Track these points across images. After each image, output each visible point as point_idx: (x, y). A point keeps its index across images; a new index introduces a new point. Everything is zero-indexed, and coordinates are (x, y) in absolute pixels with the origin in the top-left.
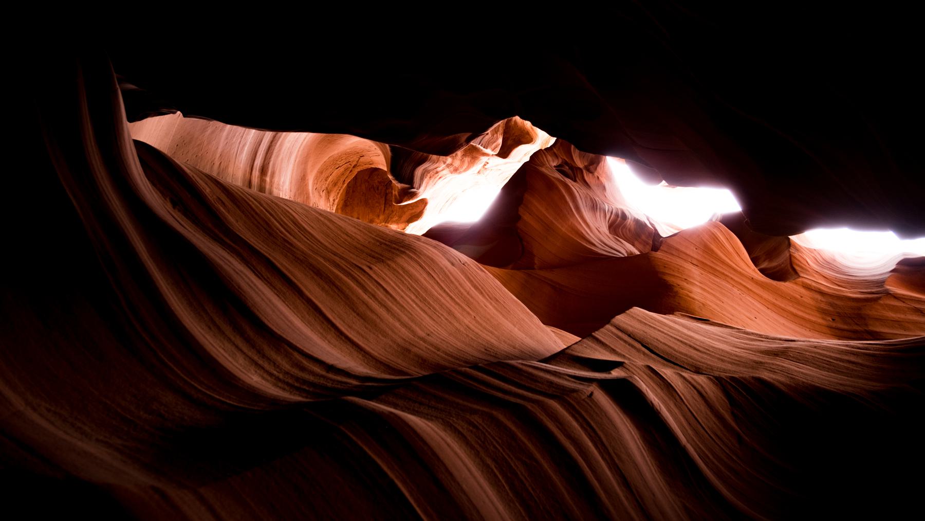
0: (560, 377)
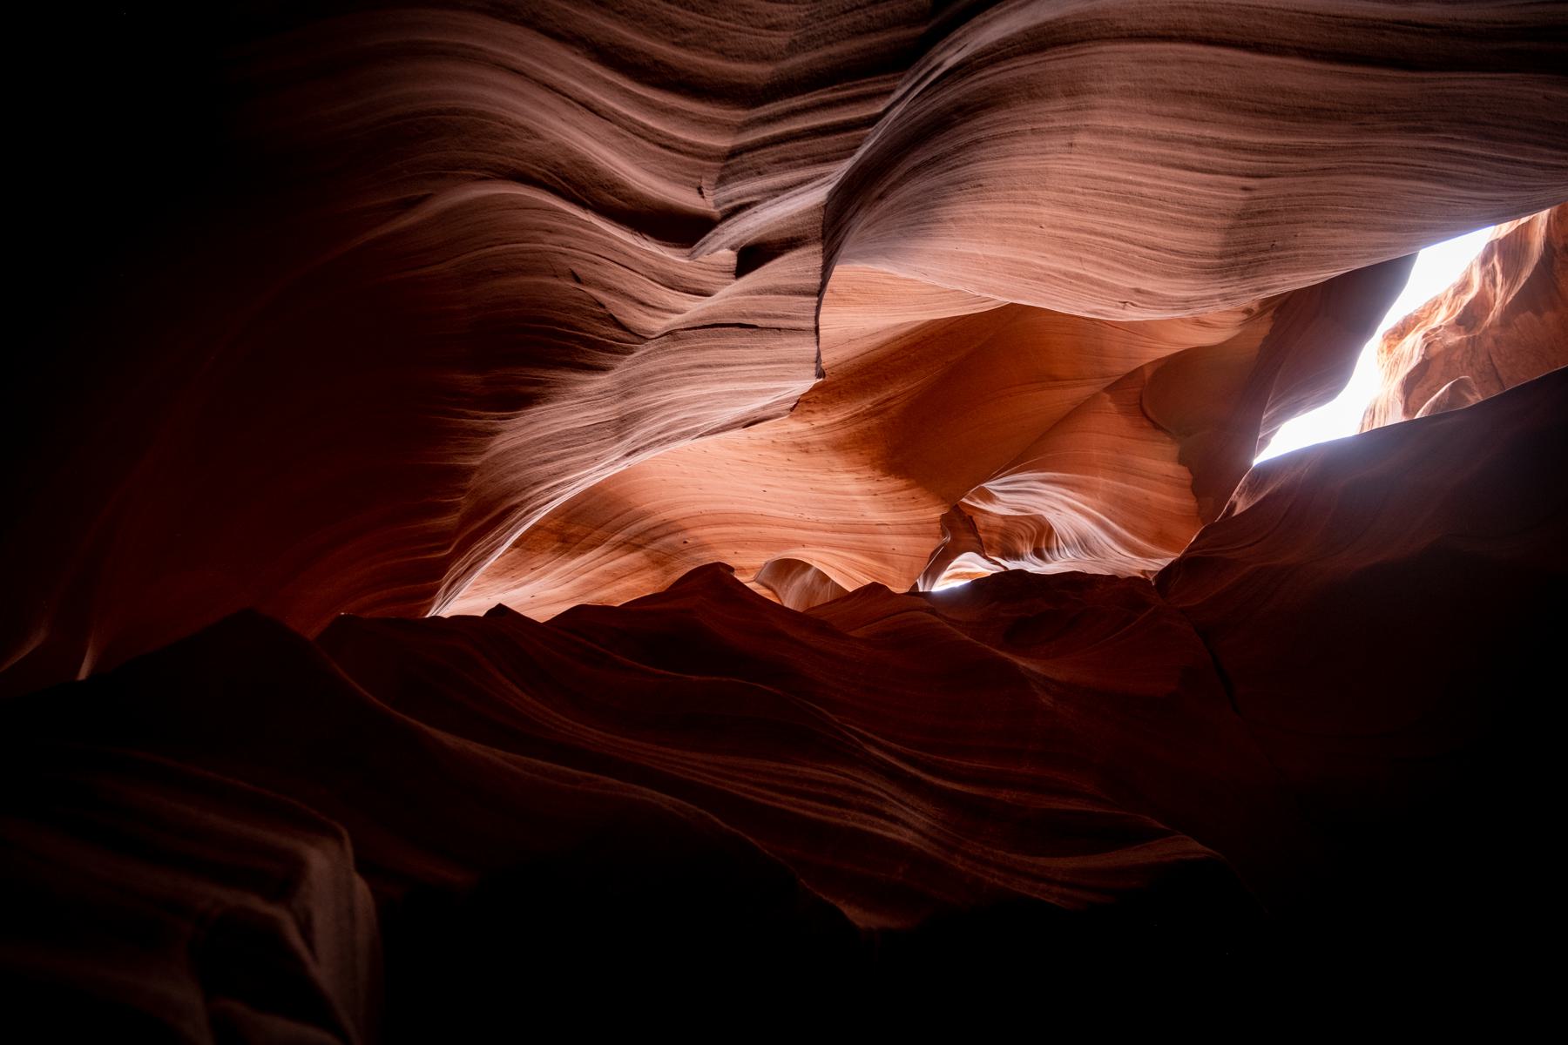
0: (763, 191)
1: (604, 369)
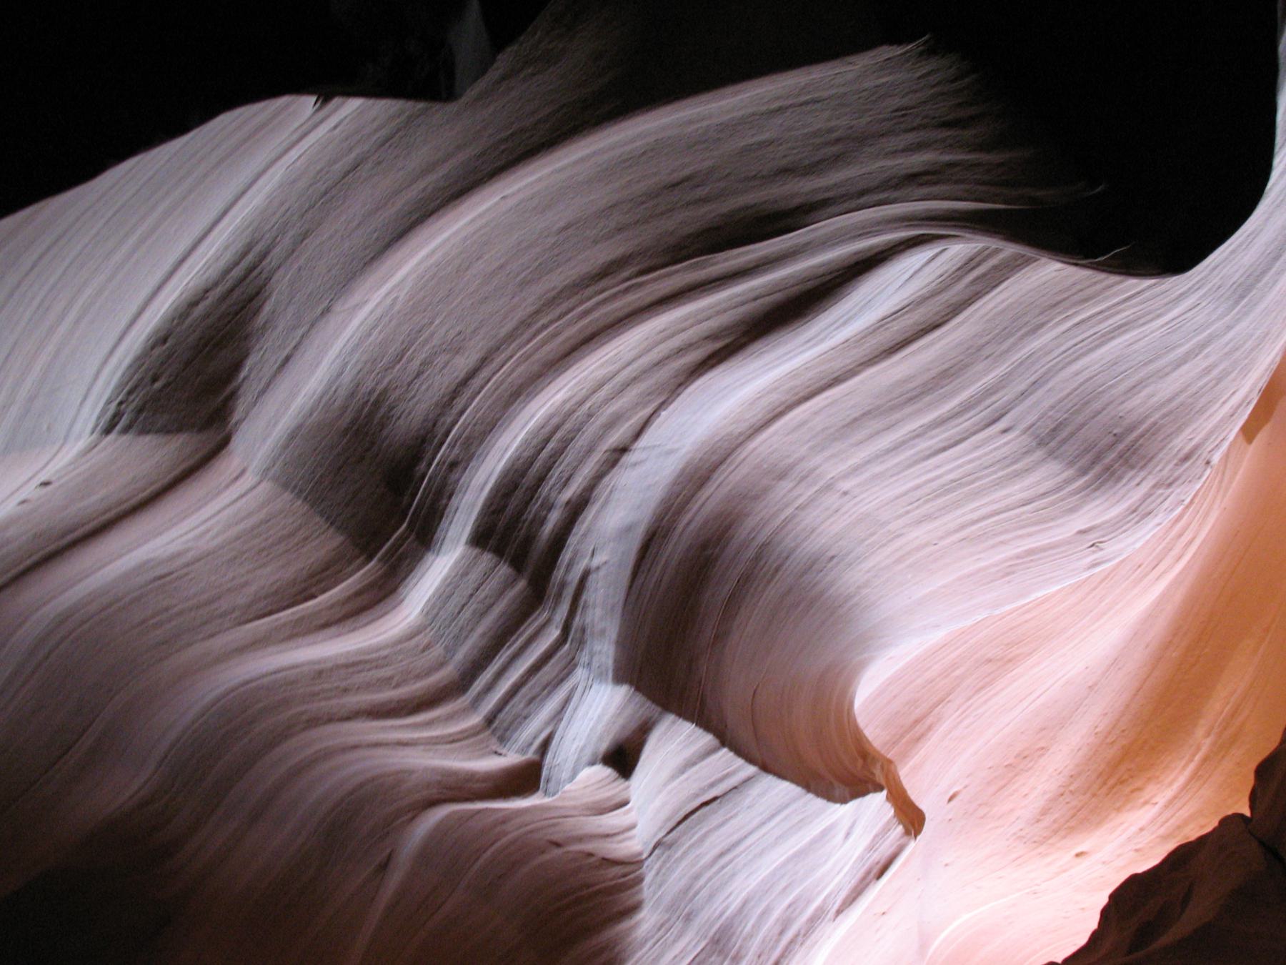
0: (547, 723)
1: (635, 908)
